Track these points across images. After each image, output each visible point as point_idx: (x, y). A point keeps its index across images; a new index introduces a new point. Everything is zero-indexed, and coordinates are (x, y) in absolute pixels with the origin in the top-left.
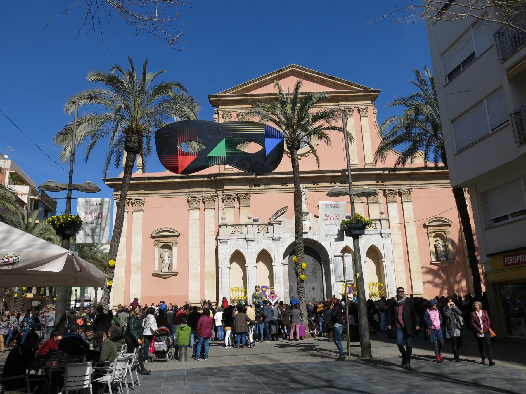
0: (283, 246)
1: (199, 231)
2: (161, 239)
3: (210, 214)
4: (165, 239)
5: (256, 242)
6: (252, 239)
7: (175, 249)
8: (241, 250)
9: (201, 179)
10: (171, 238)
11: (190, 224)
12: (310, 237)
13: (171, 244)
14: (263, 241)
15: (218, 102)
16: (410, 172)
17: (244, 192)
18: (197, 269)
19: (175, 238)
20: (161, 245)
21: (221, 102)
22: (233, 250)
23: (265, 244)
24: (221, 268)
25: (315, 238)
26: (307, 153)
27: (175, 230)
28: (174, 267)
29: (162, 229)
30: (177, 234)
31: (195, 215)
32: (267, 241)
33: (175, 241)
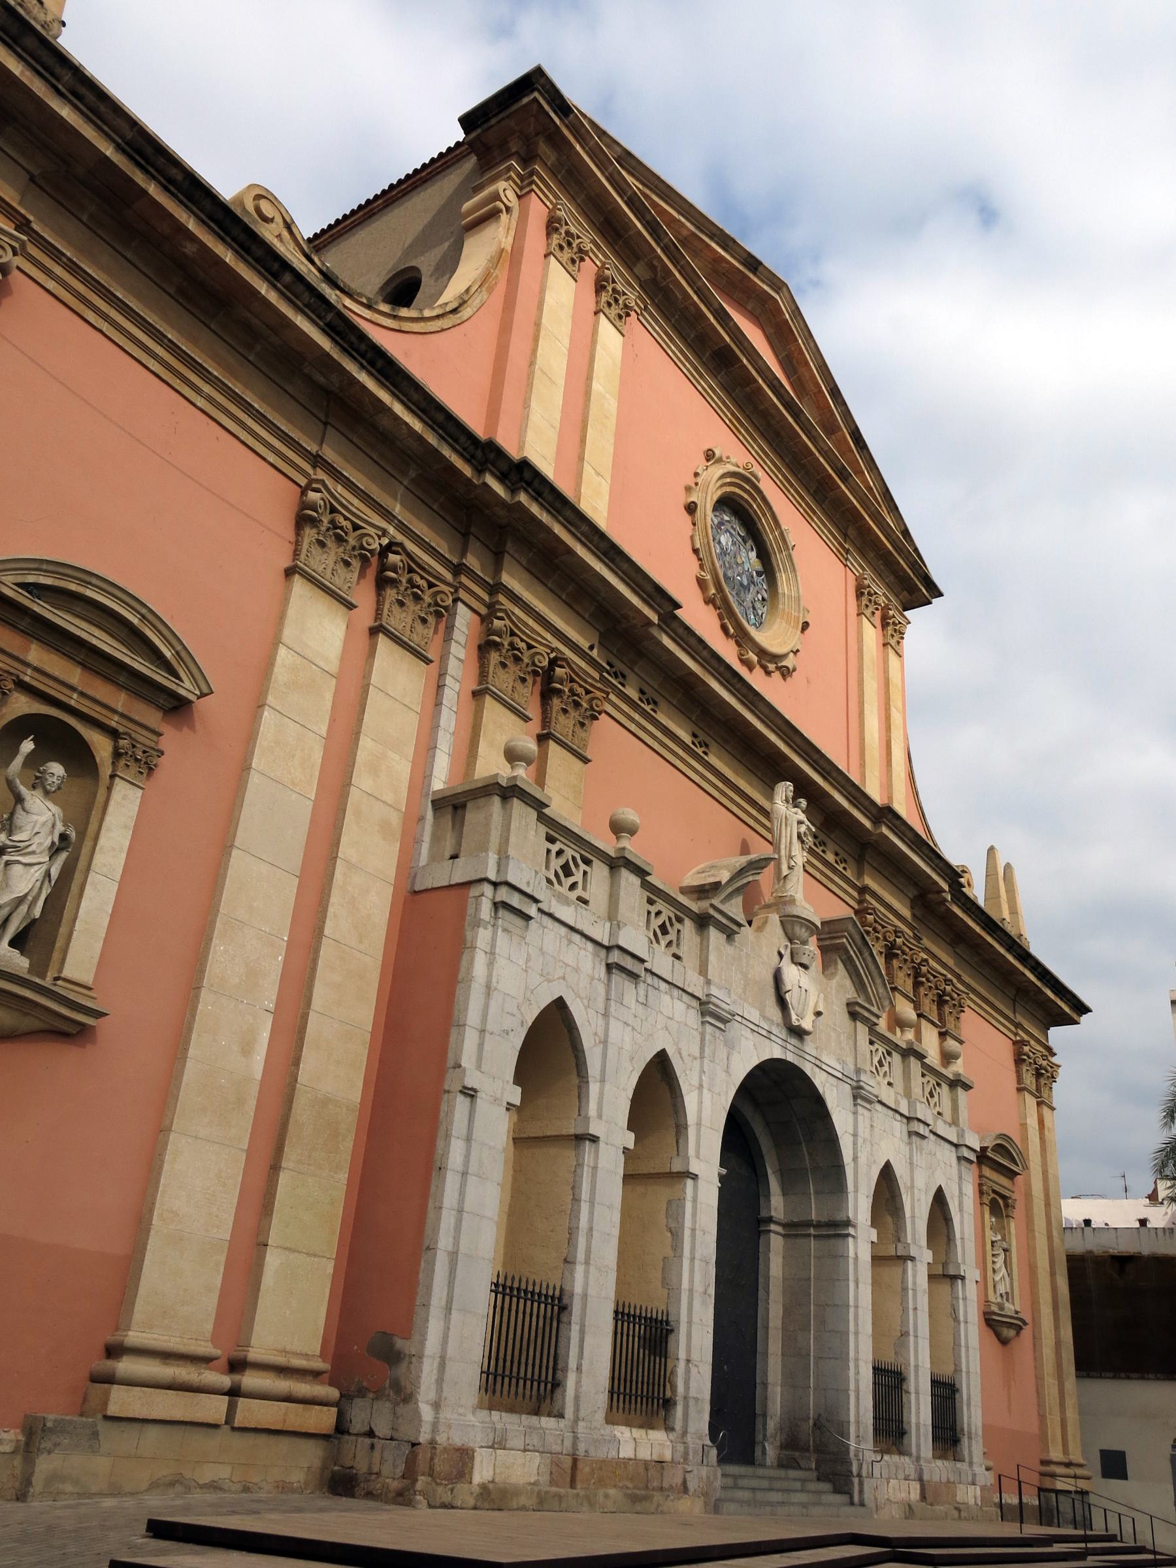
0: (727, 1071)
1: (318, 756)
2: (36, 654)
3: (396, 676)
4: (74, 675)
6: (637, 968)
7: (124, 805)
12: (808, 1069)
15: (543, 148)
18: (247, 1050)
24: (470, 1093)
25: (819, 1080)
27: (183, 654)
28: (81, 957)
30: (186, 688)
31: (318, 632)
33: (143, 737)
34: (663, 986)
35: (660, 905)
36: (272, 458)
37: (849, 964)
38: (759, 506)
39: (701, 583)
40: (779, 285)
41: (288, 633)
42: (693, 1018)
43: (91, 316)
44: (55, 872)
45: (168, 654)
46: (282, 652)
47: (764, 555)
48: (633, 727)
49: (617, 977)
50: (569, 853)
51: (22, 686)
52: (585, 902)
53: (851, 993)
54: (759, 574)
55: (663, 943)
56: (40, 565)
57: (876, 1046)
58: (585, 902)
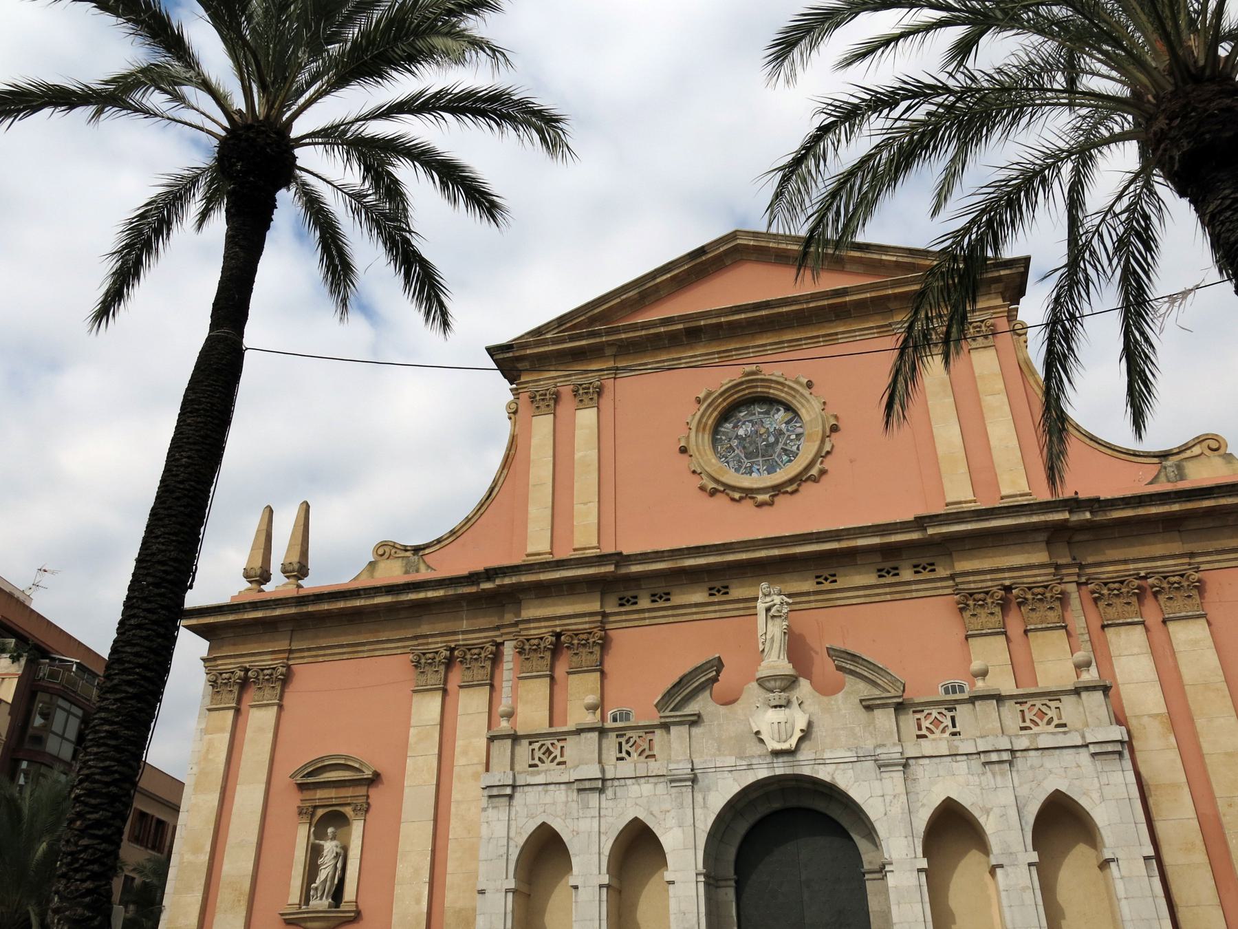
2: (320, 794)
3: (471, 705)
5: (609, 792)
7: (357, 828)
8: (557, 825)
9: (451, 592)
10: (348, 792)
11: (412, 740)
12: (807, 771)
13: (348, 810)
14: (634, 789)
15: (520, 366)
16: (1176, 507)
17: (583, 624)
18: (418, 902)
19: (362, 791)
20: (320, 812)
21: (526, 365)
22: (532, 826)
23: (638, 800)
25: (823, 774)
26: (791, 481)
27: (361, 763)
29: (322, 759)
30: (368, 774)
31: (428, 708)
32: (646, 788)
34: (629, 782)
35: (629, 734)
36: (399, 651)
37: (852, 673)
38: (762, 386)
39: (702, 488)
40: (733, 235)
41: (413, 722)
42: (662, 788)
43: (321, 659)
44: (339, 865)
45: (357, 765)
46: (412, 730)
47: (788, 408)
48: (647, 622)
49: (584, 795)
50: (548, 743)
51: (315, 807)
52: (564, 763)
53: (865, 690)
54: (787, 423)
55: (635, 755)
56: (305, 766)
57: (926, 712)
58: (564, 763)
